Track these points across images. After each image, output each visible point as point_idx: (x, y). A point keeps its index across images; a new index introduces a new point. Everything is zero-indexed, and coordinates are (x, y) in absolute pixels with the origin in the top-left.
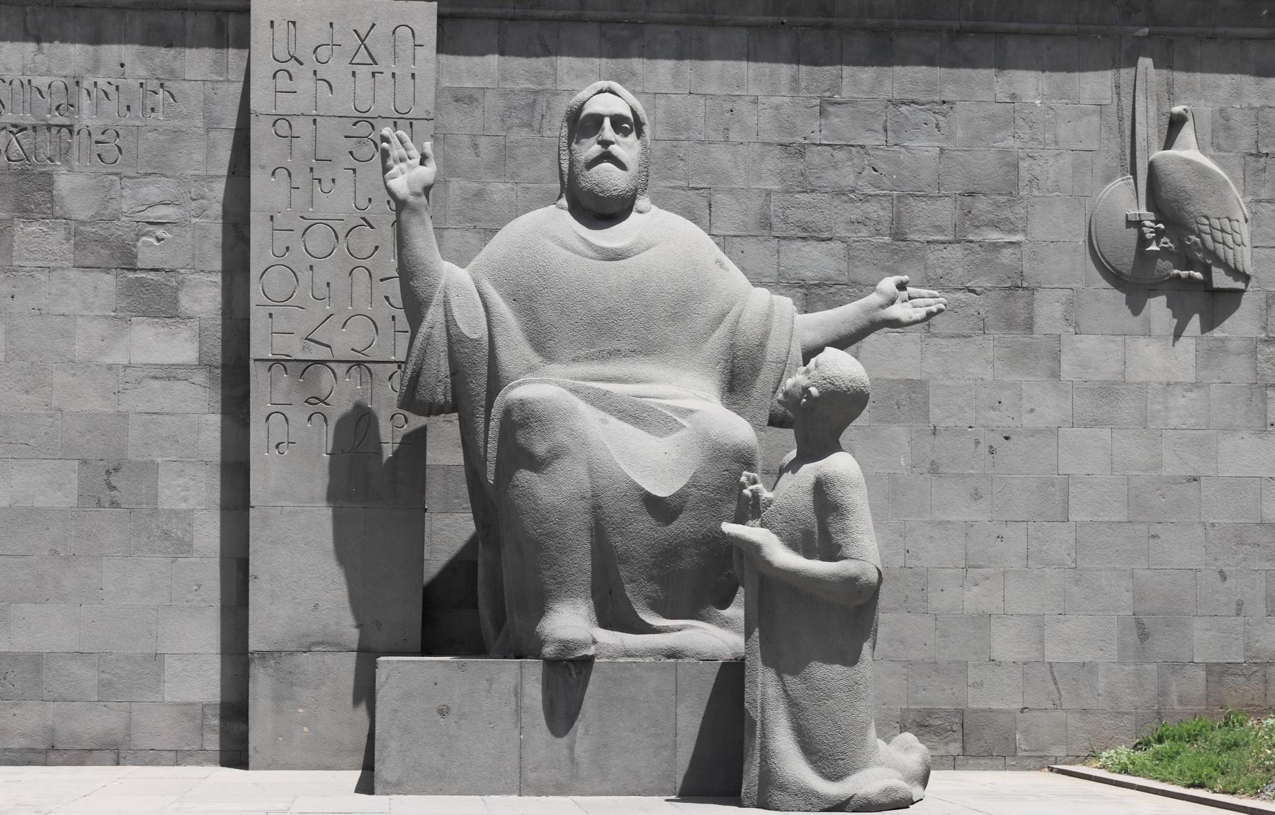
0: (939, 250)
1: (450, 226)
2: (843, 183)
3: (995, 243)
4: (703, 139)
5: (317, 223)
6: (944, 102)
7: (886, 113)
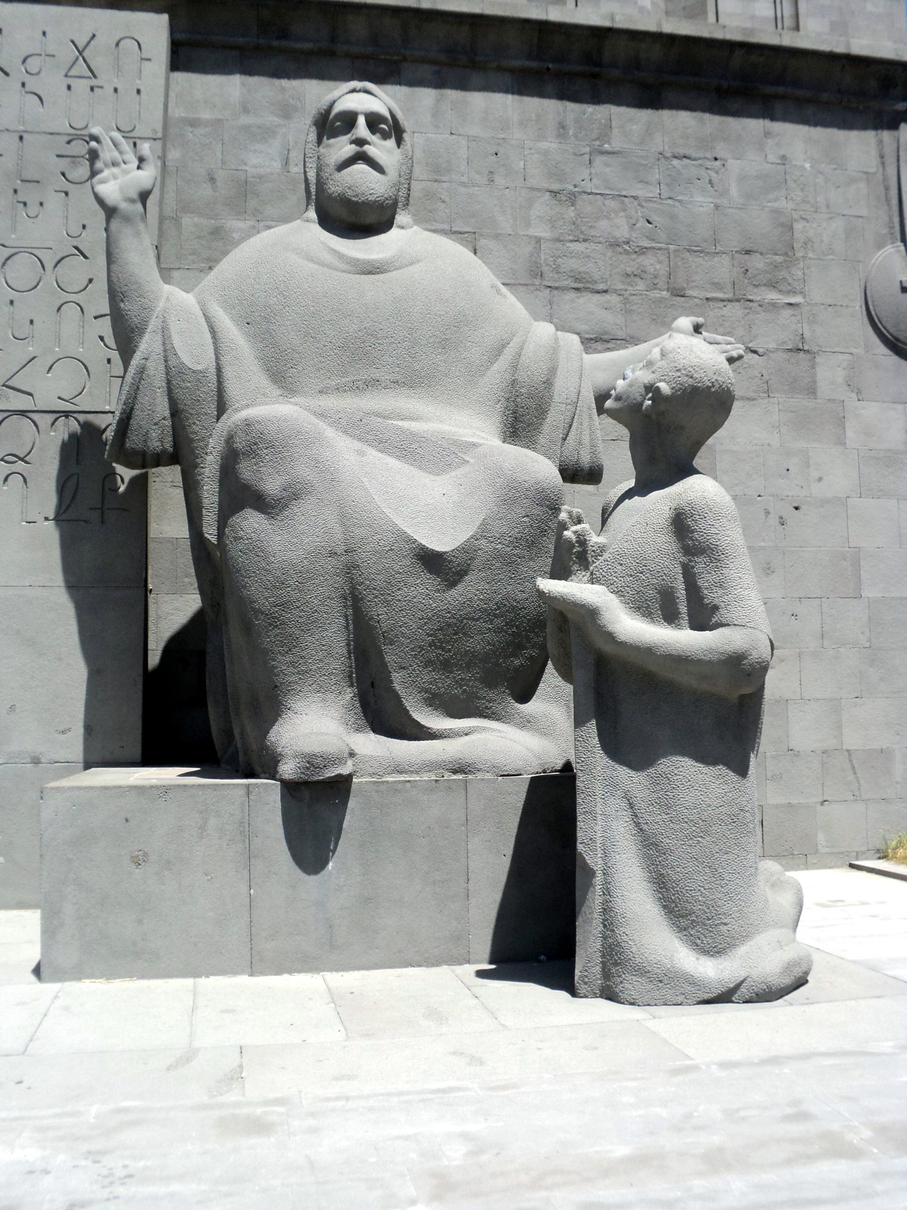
0: (719, 308)
1: (182, 266)
3: (775, 303)
4: (466, 180)
5: (20, 252)
6: (716, 159)
7: (658, 165)
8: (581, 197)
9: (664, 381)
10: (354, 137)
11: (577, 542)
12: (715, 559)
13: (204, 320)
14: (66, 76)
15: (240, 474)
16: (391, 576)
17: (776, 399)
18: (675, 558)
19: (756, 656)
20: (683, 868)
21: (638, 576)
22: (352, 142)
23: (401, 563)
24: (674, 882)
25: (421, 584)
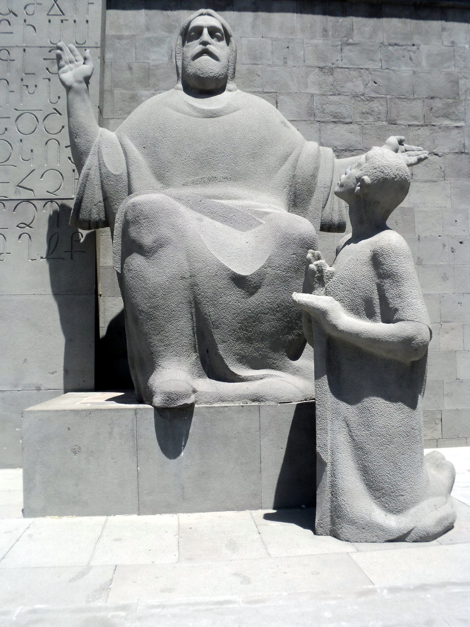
0: (416, 130)
1: (115, 117)
2: (357, 90)
3: (448, 126)
4: (271, 63)
5: (25, 113)
6: (413, 45)
7: (380, 50)
8: (336, 70)
9: (367, 175)
10: (201, 41)
11: (317, 270)
12: (396, 281)
13: (121, 146)
14: (48, 15)
15: (130, 234)
16: (216, 290)
17: (449, 181)
18: (373, 280)
19: (420, 339)
20: (377, 463)
21: (352, 291)
22: (201, 44)
23: (222, 283)
24: (372, 471)
25: (234, 294)
